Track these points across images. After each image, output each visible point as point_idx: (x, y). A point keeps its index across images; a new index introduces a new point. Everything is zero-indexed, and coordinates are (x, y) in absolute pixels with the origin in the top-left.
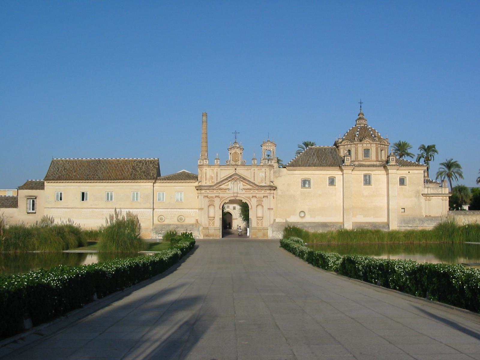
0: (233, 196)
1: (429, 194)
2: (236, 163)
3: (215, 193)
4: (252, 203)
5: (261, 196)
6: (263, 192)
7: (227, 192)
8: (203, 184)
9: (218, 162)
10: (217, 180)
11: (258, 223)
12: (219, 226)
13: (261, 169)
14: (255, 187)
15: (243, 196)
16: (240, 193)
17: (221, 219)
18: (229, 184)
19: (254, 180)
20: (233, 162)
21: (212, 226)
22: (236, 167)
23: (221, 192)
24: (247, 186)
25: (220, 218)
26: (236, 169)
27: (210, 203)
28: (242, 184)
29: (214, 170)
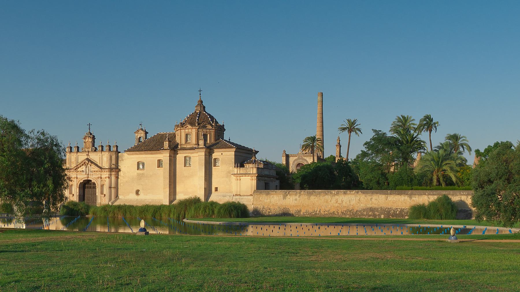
1: (238, 174)
4: (98, 183)
10: (75, 165)
19: (100, 164)
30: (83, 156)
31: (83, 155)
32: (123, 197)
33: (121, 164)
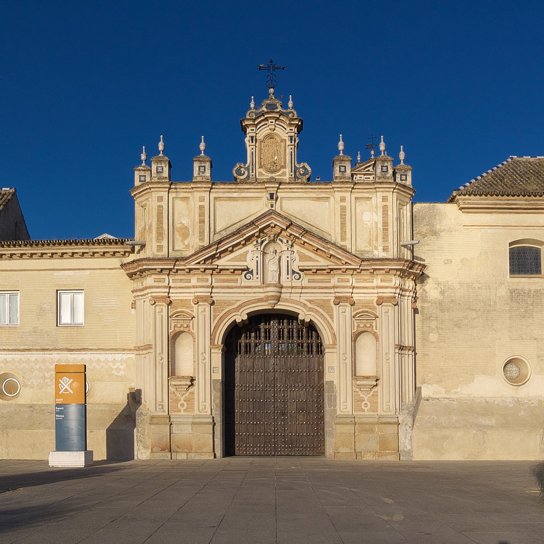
0: (262, 295)
3: (194, 287)
4: (334, 325)
5: (367, 297)
6: (377, 281)
7: (241, 280)
8: (147, 253)
9: (203, 173)
10: (202, 239)
11: (357, 401)
13: (369, 199)
15: (303, 298)
17: (219, 386)
19: (343, 239)
24: (317, 261)
26: (272, 197)
29: (191, 199)
31: (243, 195)
32: (443, 391)
33: (426, 248)
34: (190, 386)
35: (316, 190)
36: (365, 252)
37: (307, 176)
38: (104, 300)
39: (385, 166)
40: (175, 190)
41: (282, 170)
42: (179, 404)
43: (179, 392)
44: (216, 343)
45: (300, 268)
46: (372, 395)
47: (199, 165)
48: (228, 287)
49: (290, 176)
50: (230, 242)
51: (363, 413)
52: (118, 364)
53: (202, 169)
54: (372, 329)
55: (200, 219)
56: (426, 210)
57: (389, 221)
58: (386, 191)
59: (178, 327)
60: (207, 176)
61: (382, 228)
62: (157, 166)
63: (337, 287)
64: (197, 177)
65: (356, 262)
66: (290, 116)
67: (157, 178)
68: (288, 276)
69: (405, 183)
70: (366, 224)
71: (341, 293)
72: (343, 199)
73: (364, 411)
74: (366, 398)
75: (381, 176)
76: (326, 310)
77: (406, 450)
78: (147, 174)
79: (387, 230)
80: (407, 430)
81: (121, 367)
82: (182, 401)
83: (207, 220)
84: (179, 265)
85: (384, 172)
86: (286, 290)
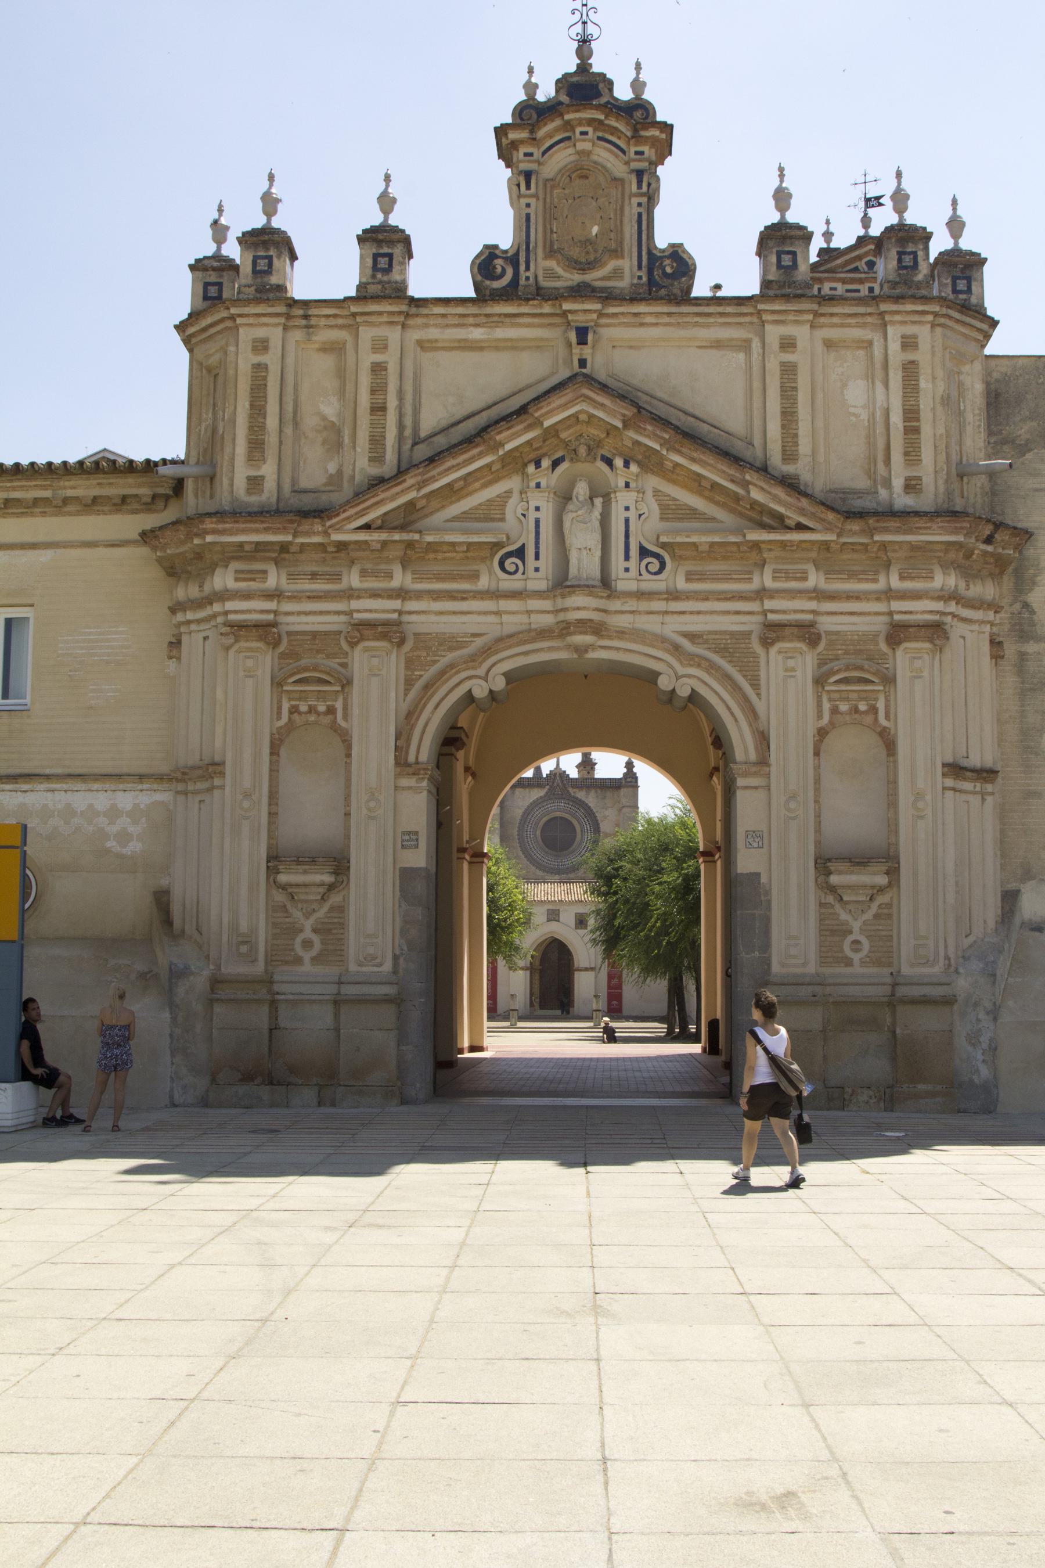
0: (548, 620)
2: (593, 277)
12: (388, 966)
14: (800, 527)
16: (632, 586)
18: (509, 493)
20: (552, 264)
21: (315, 960)
22: (583, 310)
23: (419, 578)
25: (407, 874)
27: (294, 710)
28: (656, 492)
30: (488, 357)
34: (331, 887)
35: (712, 320)
36: (855, 493)
37: (684, 279)
38: (90, 634)
39: (910, 253)
40: (304, 322)
41: (611, 265)
42: (299, 940)
43: (300, 905)
44: (411, 758)
45: (664, 539)
46: (876, 916)
47: (374, 251)
48: (452, 596)
49: (635, 281)
50: (459, 467)
51: (849, 970)
52: (124, 822)
53: (383, 262)
54: (876, 719)
55: (374, 401)
56: (1027, 377)
57: (922, 407)
58: (914, 323)
59: (300, 713)
60: (396, 282)
61: (901, 425)
62: (254, 257)
63: (772, 594)
64: (369, 283)
65: (829, 523)
66: (635, 117)
67: (253, 289)
68: (627, 564)
69: (965, 300)
70: (854, 415)
71: (784, 612)
72: (788, 344)
73: (849, 963)
74: (856, 926)
75: (898, 279)
76: (740, 664)
77: (977, 1081)
78: (226, 278)
79: (917, 430)
80: (978, 1020)
81: (131, 829)
82: (308, 934)
83: (392, 403)
84: (308, 534)
85: (906, 268)
86: (622, 605)
